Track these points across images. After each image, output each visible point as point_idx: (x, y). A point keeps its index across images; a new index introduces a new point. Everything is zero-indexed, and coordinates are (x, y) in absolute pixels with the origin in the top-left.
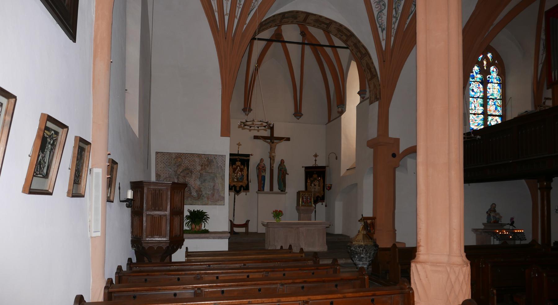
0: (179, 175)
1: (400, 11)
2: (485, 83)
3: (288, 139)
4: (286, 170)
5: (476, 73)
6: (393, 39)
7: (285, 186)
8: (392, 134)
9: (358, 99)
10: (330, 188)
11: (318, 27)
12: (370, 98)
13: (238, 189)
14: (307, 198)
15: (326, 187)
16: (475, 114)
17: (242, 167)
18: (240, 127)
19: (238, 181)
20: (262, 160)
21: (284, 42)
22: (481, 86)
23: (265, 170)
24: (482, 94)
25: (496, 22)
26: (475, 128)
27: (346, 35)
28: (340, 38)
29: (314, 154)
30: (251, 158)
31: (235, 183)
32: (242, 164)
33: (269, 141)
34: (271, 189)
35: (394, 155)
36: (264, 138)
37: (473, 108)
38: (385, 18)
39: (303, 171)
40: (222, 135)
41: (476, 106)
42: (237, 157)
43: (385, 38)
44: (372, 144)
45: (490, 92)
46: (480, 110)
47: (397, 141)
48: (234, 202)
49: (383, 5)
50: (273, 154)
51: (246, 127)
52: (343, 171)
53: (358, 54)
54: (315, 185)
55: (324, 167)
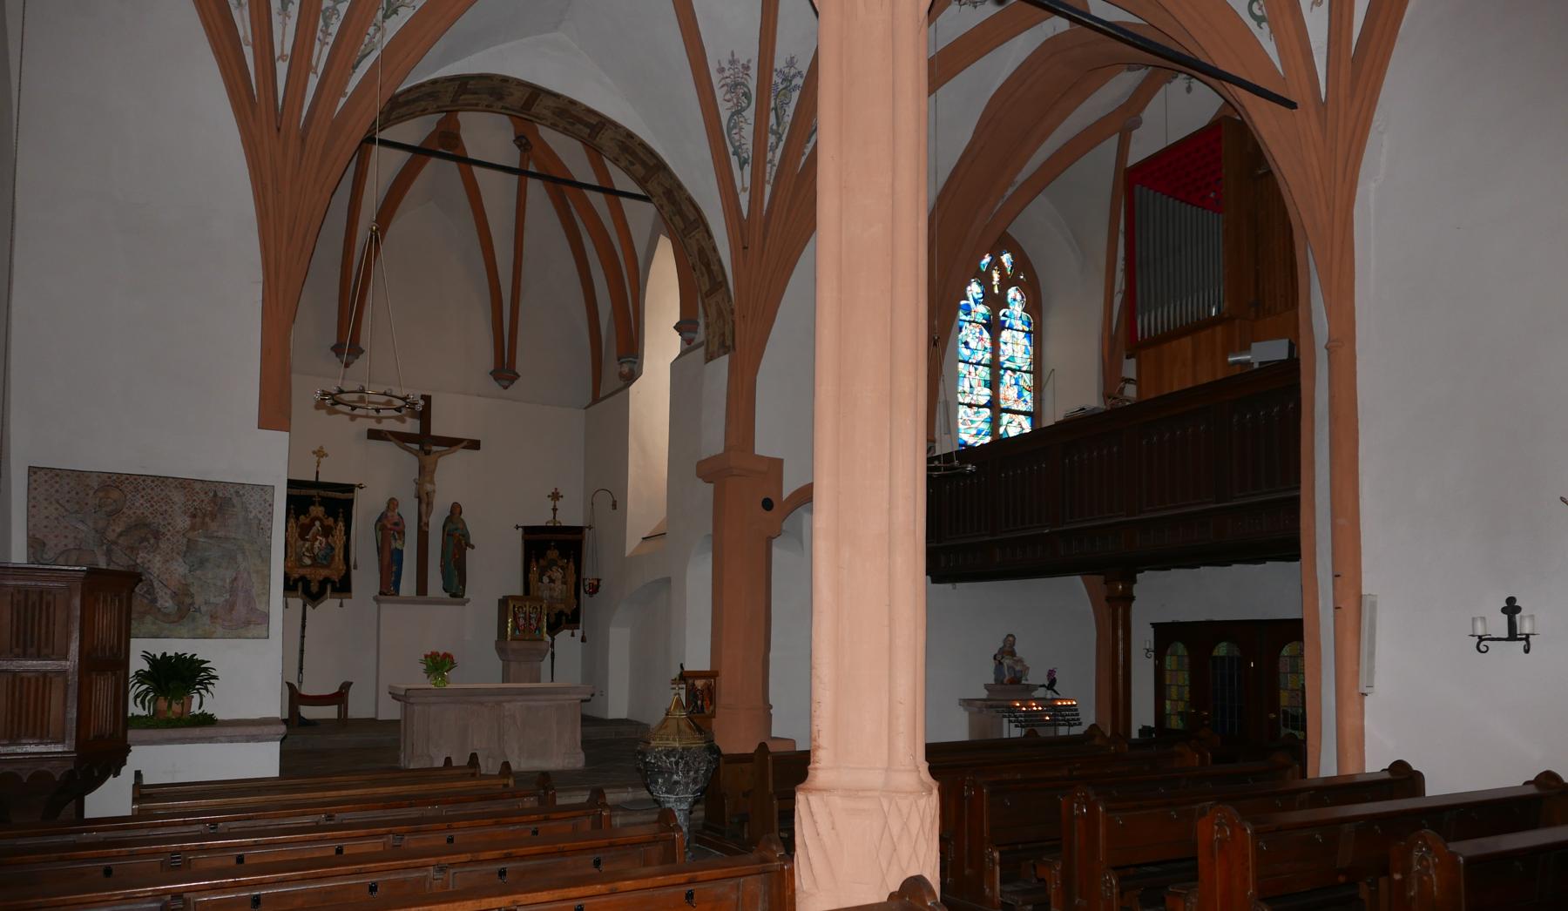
0: (115, 543)
1: (788, 119)
2: (994, 327)
3: (474, 445)
4: (466, 535)
5: (976, 302)
6: (768, 189)
7: (463, 581)
8: (764, 446)
9: (674, 344)
10: (595, 589)
11: (565, 131)
12: (706, 343)
13: (314, 588)
14: (528, 619)
15: (583, 587)
16: (970, 406)
17: (330, 521)
18: (319, 405)
19: (315, 562)
20: (392, 503)
21: (465, 162)
22: (986, 335)
23: (402, 533)
24: (988, 356)
25: (1021, 177)
26: (971, 441)
27: (644, 164)
28: (627, 171)
29: (550, 491)
30: (360, 498)
31: (302, 571)
32: (329, 513)
33: (416, 447)
34: (422, 588)
35: (768, 504)
36: (402, 438)
37: (967, 389)
38: (748, 130)
40: (264, 423)
41: (971, 384)
42: (313, 492)
43: (748, 184)
44: (710, 471)
45: (1006, 351)
46: (984, 395)
47: (777, 464)
48: (303, 627)
49: (744, 94)
50: (429, 487)
51: (339, 407)
52: (632, 543)
53: (677, 219)
54: (552, 581)
55: (579, 530)
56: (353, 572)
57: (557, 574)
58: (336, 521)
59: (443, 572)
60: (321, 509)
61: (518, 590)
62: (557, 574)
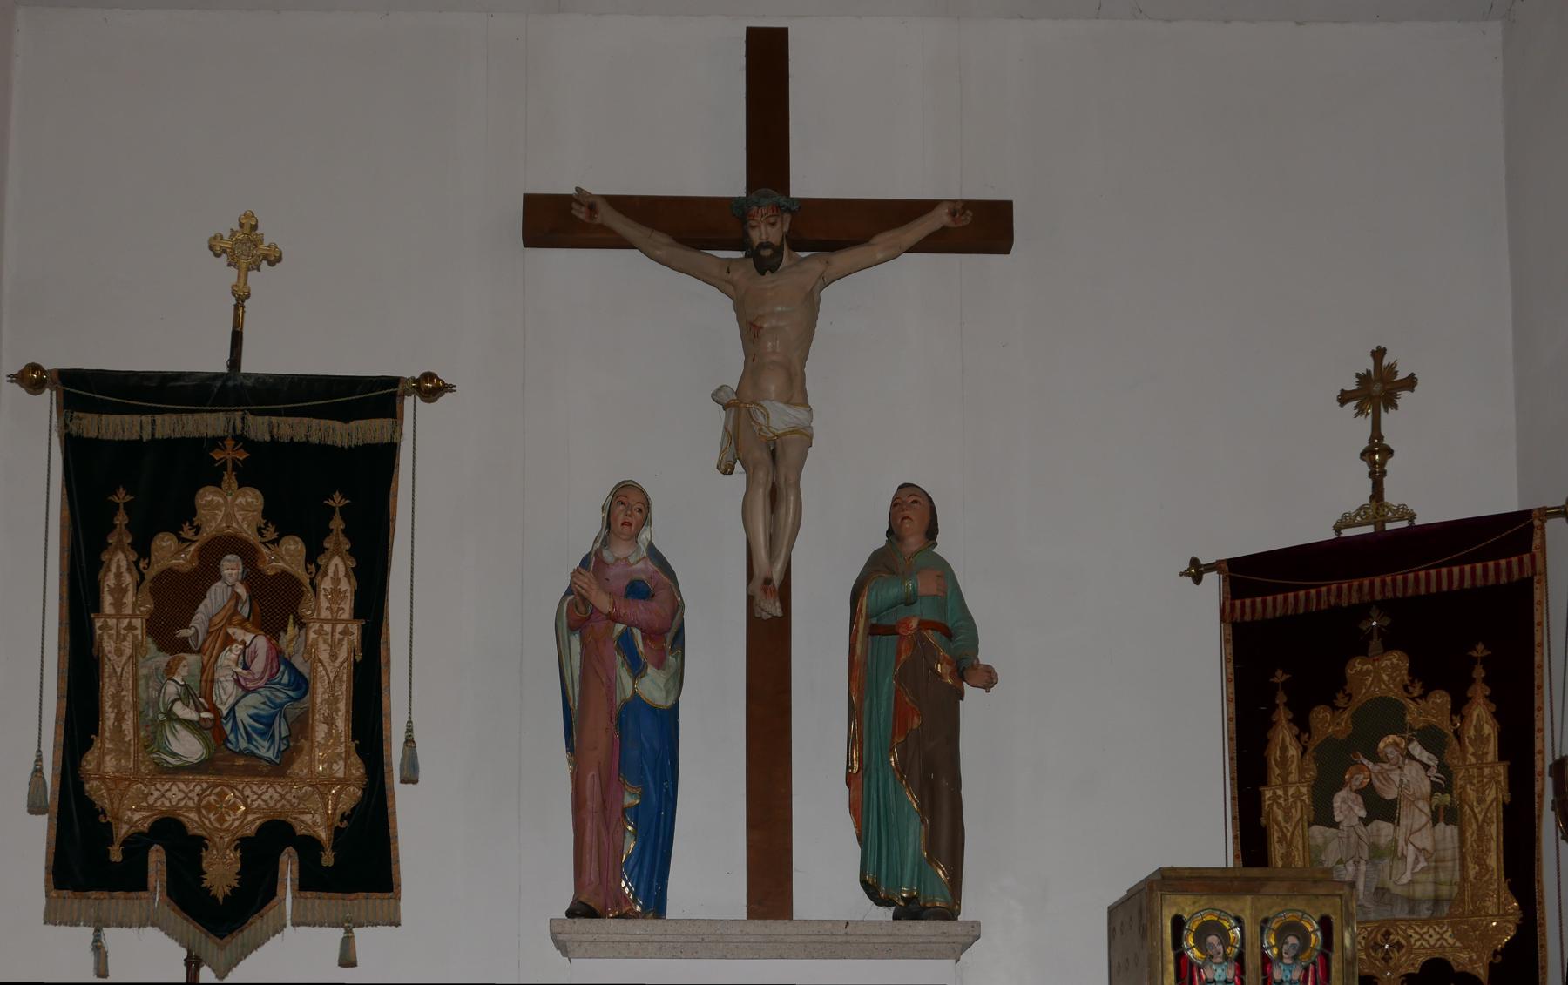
3: (984, 227)
13: (221, 871)
17: (289, 555)
19: (223, 759)
20: (627, 507)
30: (435, 466)
31: (174, 796)
32: (292, 513)
39: (1198, 629)
42: (212, 423)
50: (779, 417)
55: (1512, 534)
56: (406, 804)
57: (1407, 774)
58: (314, 553)
59: (858, 810)
60: (251, 499)
61: (1212, 847)
62: (1407, 774)
